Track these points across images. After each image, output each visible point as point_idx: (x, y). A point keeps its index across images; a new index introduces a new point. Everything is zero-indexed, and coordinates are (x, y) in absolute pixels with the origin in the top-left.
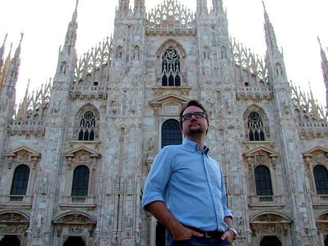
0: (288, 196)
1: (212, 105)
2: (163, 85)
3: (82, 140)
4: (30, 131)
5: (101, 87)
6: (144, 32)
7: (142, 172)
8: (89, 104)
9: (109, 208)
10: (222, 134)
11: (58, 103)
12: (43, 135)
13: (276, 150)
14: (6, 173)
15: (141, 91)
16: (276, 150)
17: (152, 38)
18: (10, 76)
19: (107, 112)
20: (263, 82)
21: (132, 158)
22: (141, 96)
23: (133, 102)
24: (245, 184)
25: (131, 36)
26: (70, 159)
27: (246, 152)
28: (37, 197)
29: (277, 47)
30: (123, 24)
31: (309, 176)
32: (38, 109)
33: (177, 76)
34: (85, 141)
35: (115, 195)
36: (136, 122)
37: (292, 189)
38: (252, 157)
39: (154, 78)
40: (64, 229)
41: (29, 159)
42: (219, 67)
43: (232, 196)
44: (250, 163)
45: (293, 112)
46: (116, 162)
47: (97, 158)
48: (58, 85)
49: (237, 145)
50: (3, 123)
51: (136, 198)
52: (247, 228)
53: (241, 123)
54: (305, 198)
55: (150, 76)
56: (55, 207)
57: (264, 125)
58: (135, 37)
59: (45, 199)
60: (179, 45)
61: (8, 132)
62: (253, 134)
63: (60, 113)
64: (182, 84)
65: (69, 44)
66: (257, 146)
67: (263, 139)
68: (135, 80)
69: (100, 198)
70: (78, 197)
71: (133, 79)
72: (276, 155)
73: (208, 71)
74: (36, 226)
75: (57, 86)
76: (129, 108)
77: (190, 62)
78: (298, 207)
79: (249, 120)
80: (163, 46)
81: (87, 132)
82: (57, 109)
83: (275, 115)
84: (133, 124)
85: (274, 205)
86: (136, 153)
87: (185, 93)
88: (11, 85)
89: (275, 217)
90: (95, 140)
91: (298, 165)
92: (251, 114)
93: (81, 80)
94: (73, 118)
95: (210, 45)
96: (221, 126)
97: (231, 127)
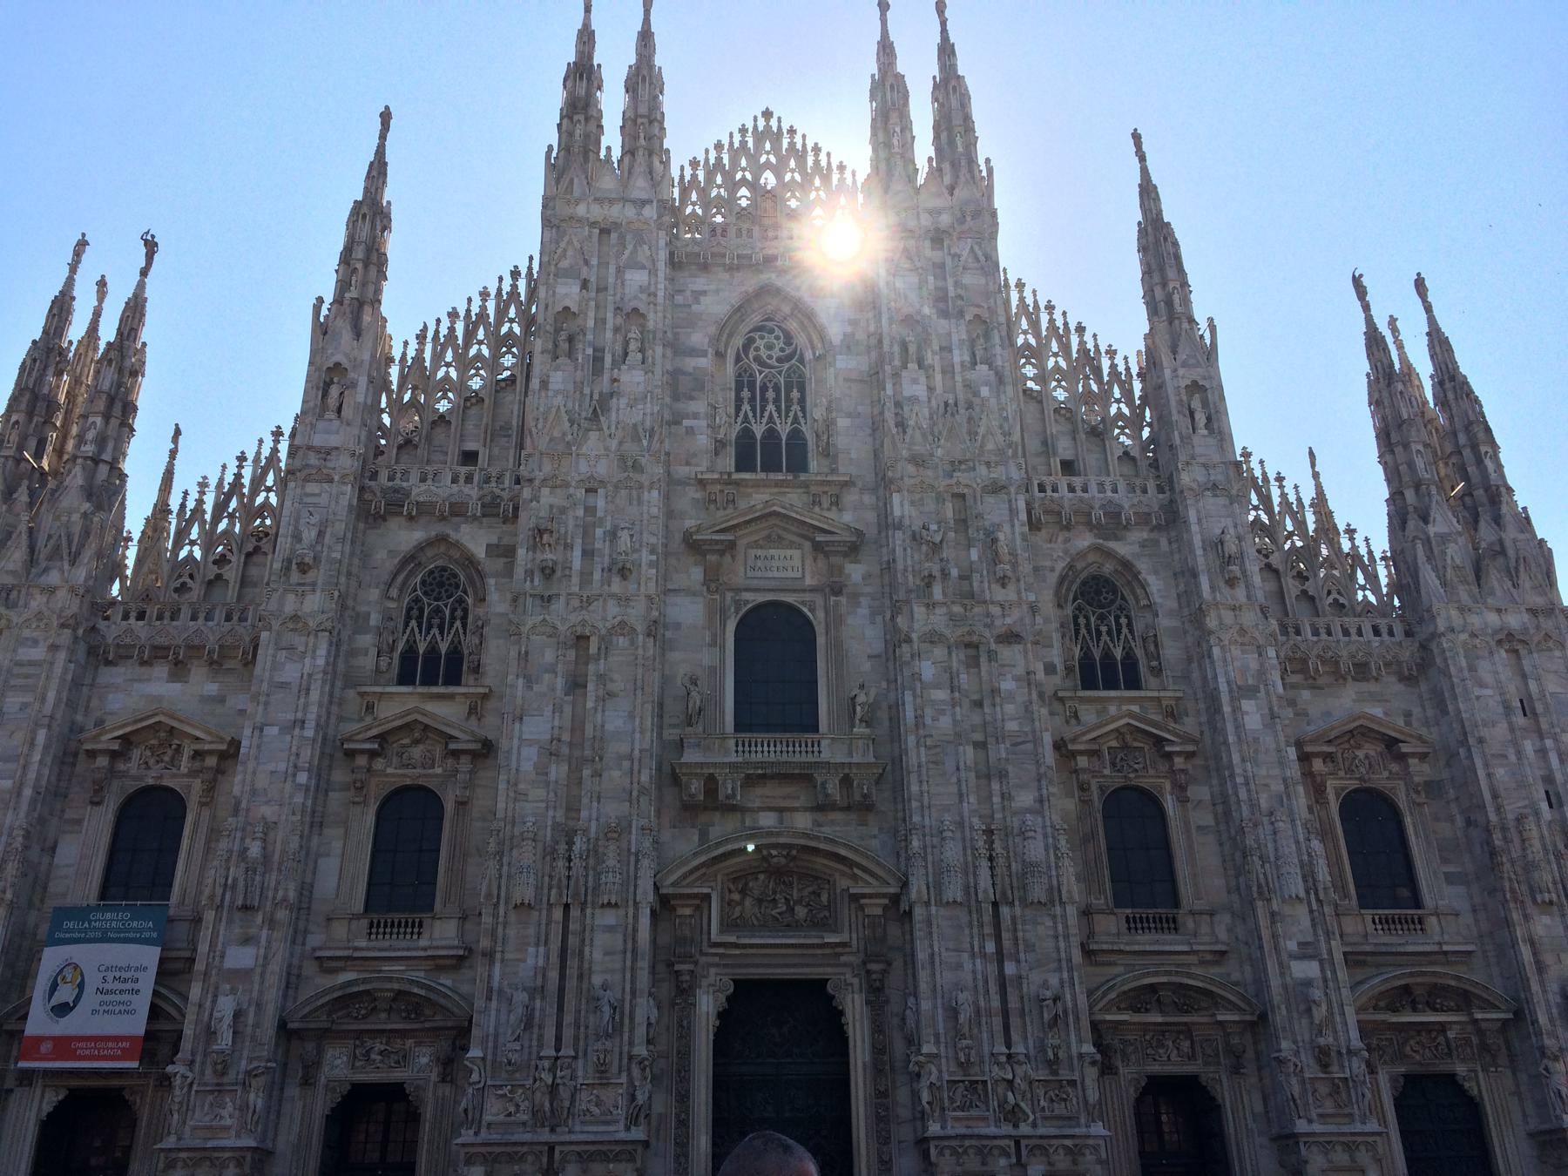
1: (936, 547)
3: (411, 682)
4: (190, 647)
5: (494, 472)
6: (663, 255)
7: (659, 813)
8: (442, 539)
9: (525, 958)
10: (974, 663)
11: (314, 534)
12: (250, 660)
13: (1190, 725)
14: (79, 822)
15: (655, 493)
16: (1190, 725)
17: (700, 283)
18: (99, 420)
19: (519, 572)
20: (1133, 459)
22: (655, 511)
23: (624, 536)
24: (1067, 862)
25: (612, 269)
26: (362, 761)
27: (1069, 732)
28: (218, 920)
29: (1192, 321)
30: (579, 221)
31: (1325, 834)
32: (223, 556)
34: (420, 689)
35: (550, 905)
36: (636, 614)
37: (1260, 886)
38: (1092, 753)
39: (703, 440)
40: (330, 1053)
41: (185, 764)
42: (961, 403)
43: (1018, 910)
44: (1084, 777)
45: (1257, 579)
46: (558, 771)
47: (474, 755)
48: (313, 460)
49: (1035, 708)
50: (69, 613)
51: (636, 917)
52: (1080, 1041)
53: (1047, 620)
54: (1314, 925)
55: (690, 431)
56: (295, 962)
57: (1139, 627)
59: (253, 931)
61: (92, 651)
62: (1093, 665)
63: (319, 575)
64: (813, 464)
65: (353, 293)
66: (1113, 710)
68: (630, 448)
69: (487, 919)
70: (396, 916)
71: (621, 443)
72: (1190, 748)
73: (919, 416)
74: (208, 1043)
75: (304, 458)
76: (607, 560)
77: (846, 380)
78: (1285, 957)
79: (1079, 608)
80: (740, 311)
81: (433, 651)
82: (307, 560)
83: (1182, 588)
84: (623, 624)
85: (1186, 948)
86: (637, 735)
87: (826, 502)
88: (107, 456)
89: (1187, 997)
91: (1277, 787)
92: (1084, 583)
93: (408, 442)
94: (374, 594)
95: (927, 310)
96: (969, 633)
97: (1011, 637)
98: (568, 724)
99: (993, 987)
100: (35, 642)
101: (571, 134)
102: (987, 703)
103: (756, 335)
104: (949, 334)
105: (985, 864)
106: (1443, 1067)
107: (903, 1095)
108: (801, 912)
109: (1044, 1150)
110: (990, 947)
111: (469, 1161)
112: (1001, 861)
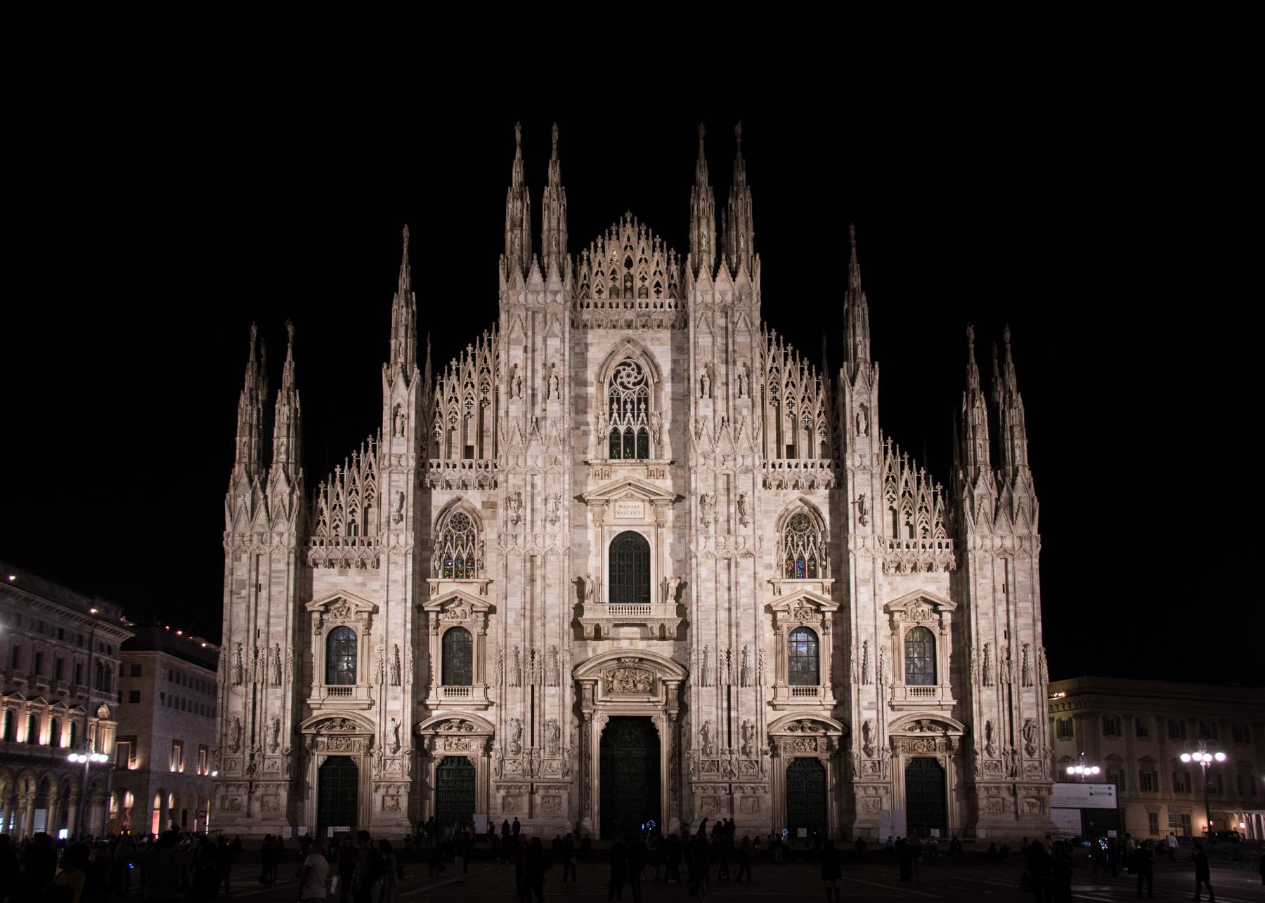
0: (848, 689)
2: (611, 457)
5: (482, 462)
15: (567, 477)
21: (553, 617)
31: (895, 649)
33: (643, 430)
39: (592, 439)
58: (549, 342)
60: (645, 353)
65: (401, 360)
66: (799, 588)
67: (813, 574)
80: (612, 354)
81: (459, 558)
90: (482, 578)
97: (748, 554)
98: (528, 600)
99: (725, 722)
100: (279, 561)
101: (513, 243)
102: (733, 588)
103: (621, 368)
104: (727, 375)
105: (726, 667)
106: (931, 755)
107: (684, 765)
108: (640, 686)
109: (741, 788)
110: (725, 705)
111: (498, 788)
112: (734, 666)
